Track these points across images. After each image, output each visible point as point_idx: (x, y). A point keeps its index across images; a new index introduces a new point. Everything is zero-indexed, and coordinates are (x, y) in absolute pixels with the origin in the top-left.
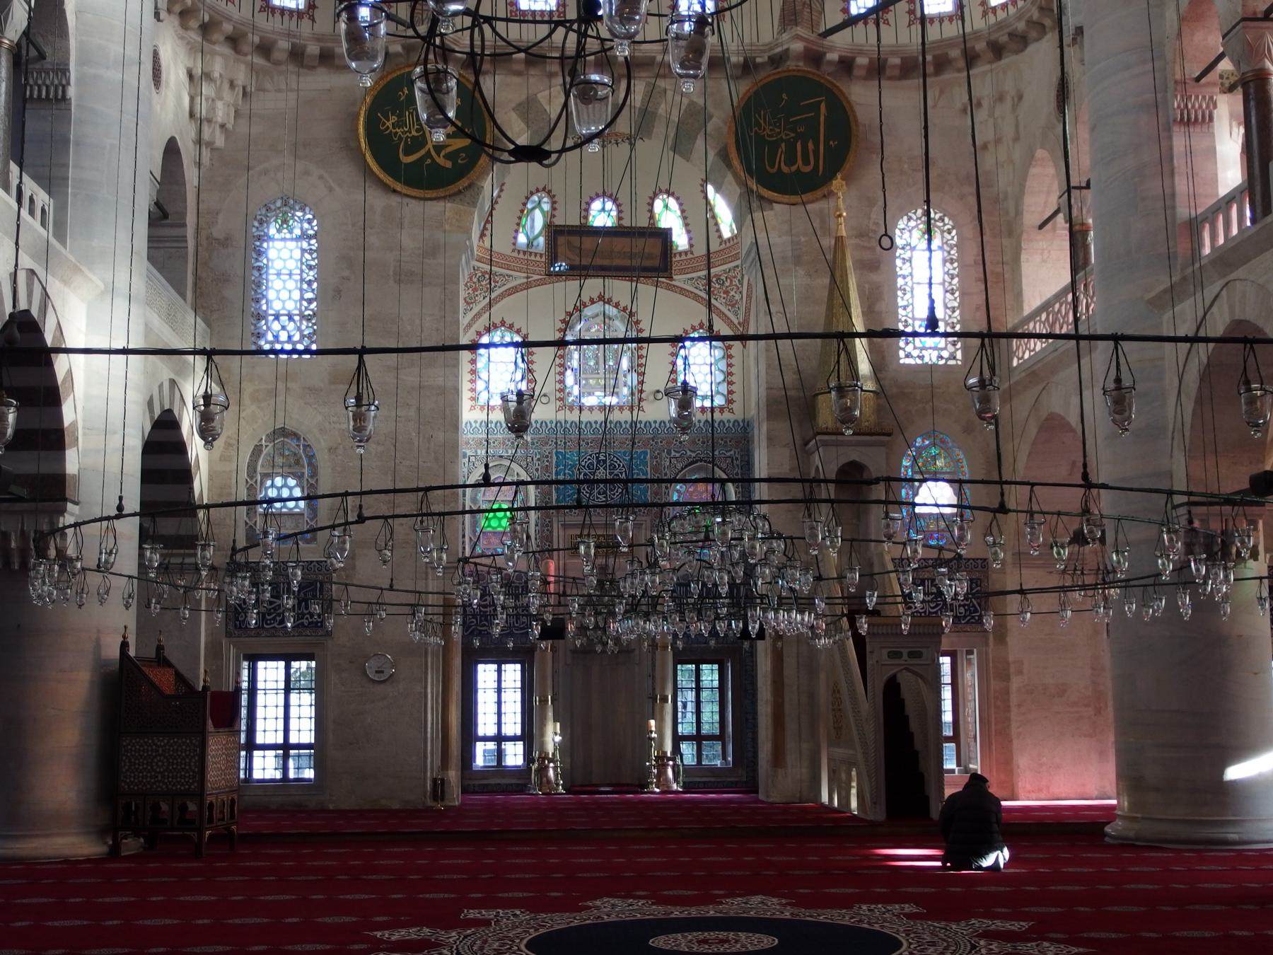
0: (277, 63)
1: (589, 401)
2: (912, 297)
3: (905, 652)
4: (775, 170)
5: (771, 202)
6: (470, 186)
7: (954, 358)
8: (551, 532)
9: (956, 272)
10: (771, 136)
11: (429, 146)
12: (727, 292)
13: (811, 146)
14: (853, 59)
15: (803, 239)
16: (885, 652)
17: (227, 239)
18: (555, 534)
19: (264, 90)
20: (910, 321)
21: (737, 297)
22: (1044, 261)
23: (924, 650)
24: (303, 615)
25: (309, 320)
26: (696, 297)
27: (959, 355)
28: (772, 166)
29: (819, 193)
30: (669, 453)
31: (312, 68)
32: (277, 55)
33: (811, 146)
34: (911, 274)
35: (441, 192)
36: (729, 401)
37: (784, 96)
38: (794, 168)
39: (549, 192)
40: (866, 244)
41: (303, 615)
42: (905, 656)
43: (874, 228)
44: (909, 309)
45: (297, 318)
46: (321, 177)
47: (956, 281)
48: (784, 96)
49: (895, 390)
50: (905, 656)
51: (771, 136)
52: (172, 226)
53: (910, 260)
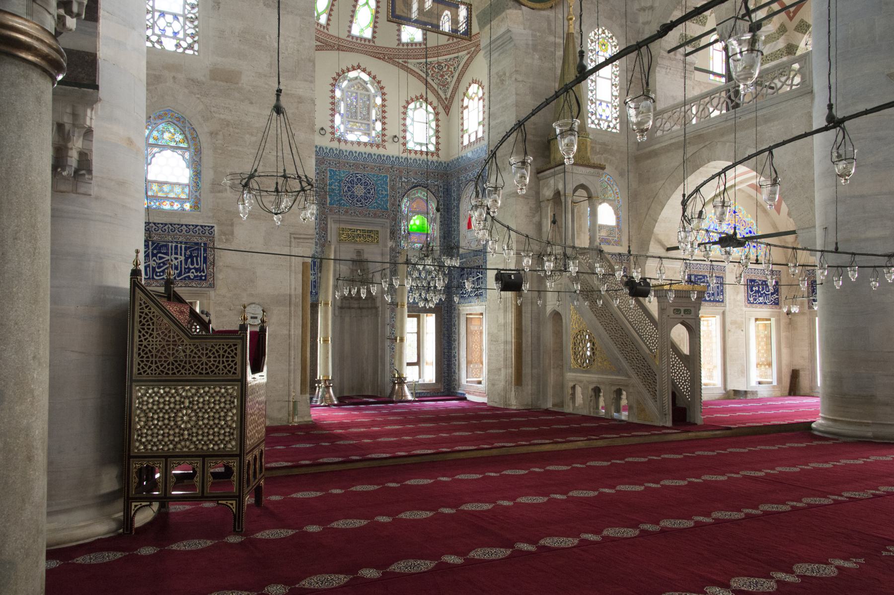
1: (351, 137)
3: (682, 309)
8: (326, 225)
9: (617, 73)
12: (442, 76)
18: (329, 226)
21: (449, 80)
22: (666, 74)
24: (190, 269)
25: (192, 22)
26: (419, 77)
27: (618, 126)
30: (401, 178)
36: (437, 149)
41: (190, 269)
45: (181, 19)
47: (617, 79)
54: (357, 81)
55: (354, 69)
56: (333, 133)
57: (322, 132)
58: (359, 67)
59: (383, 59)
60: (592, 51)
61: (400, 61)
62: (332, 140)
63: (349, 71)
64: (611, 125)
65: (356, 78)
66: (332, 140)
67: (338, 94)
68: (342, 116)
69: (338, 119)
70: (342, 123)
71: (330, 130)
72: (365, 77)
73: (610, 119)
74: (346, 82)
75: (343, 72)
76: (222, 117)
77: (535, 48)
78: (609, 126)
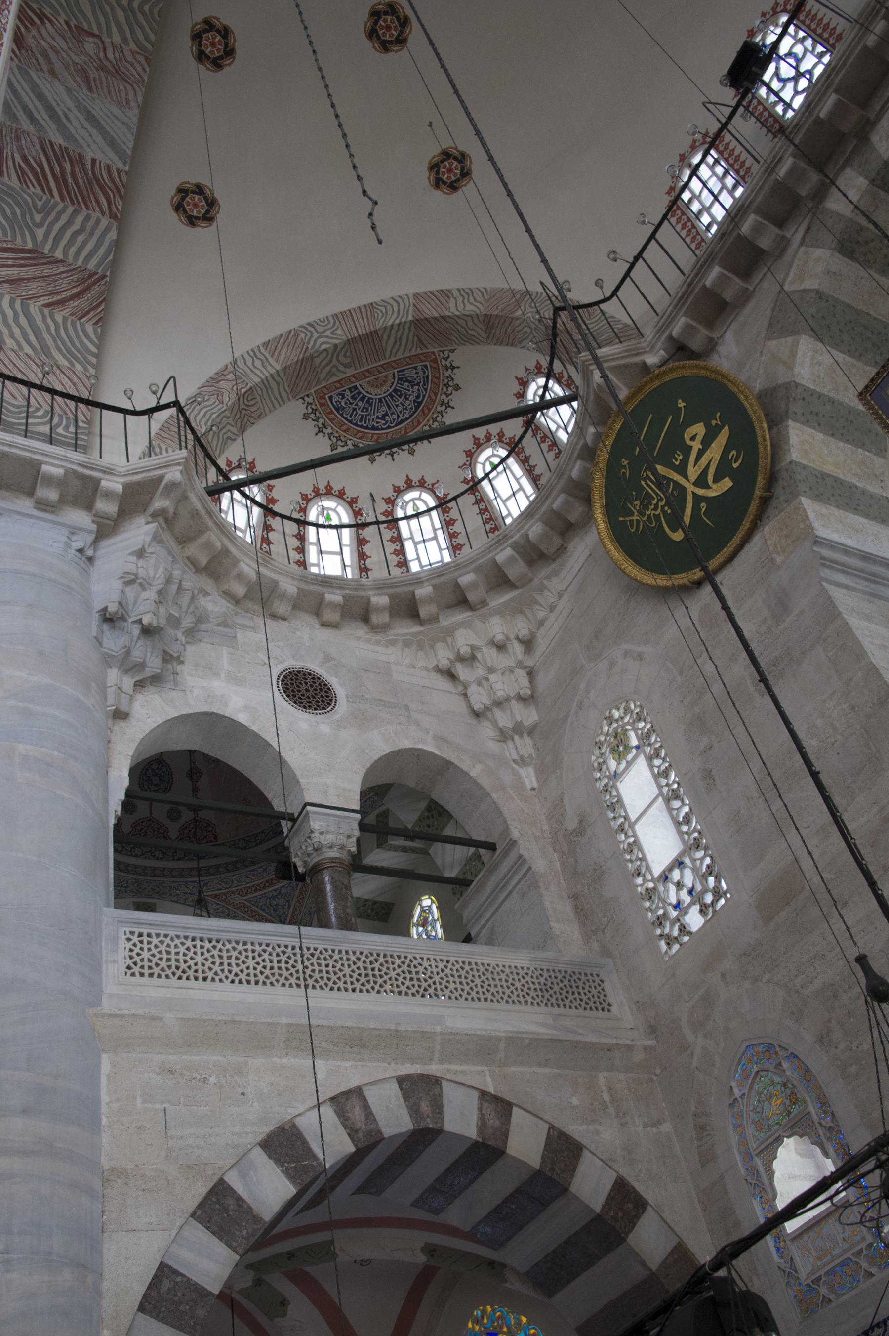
0: (526, 581)
6: (772, 479)
11: (690, 488)
17: (581, 822)
19: (541, 623)
31: (561, 550)
32: (512, 573)
35: (746, 524)
46: (626, 653)
52: (506, 853)
76: (818, 984)
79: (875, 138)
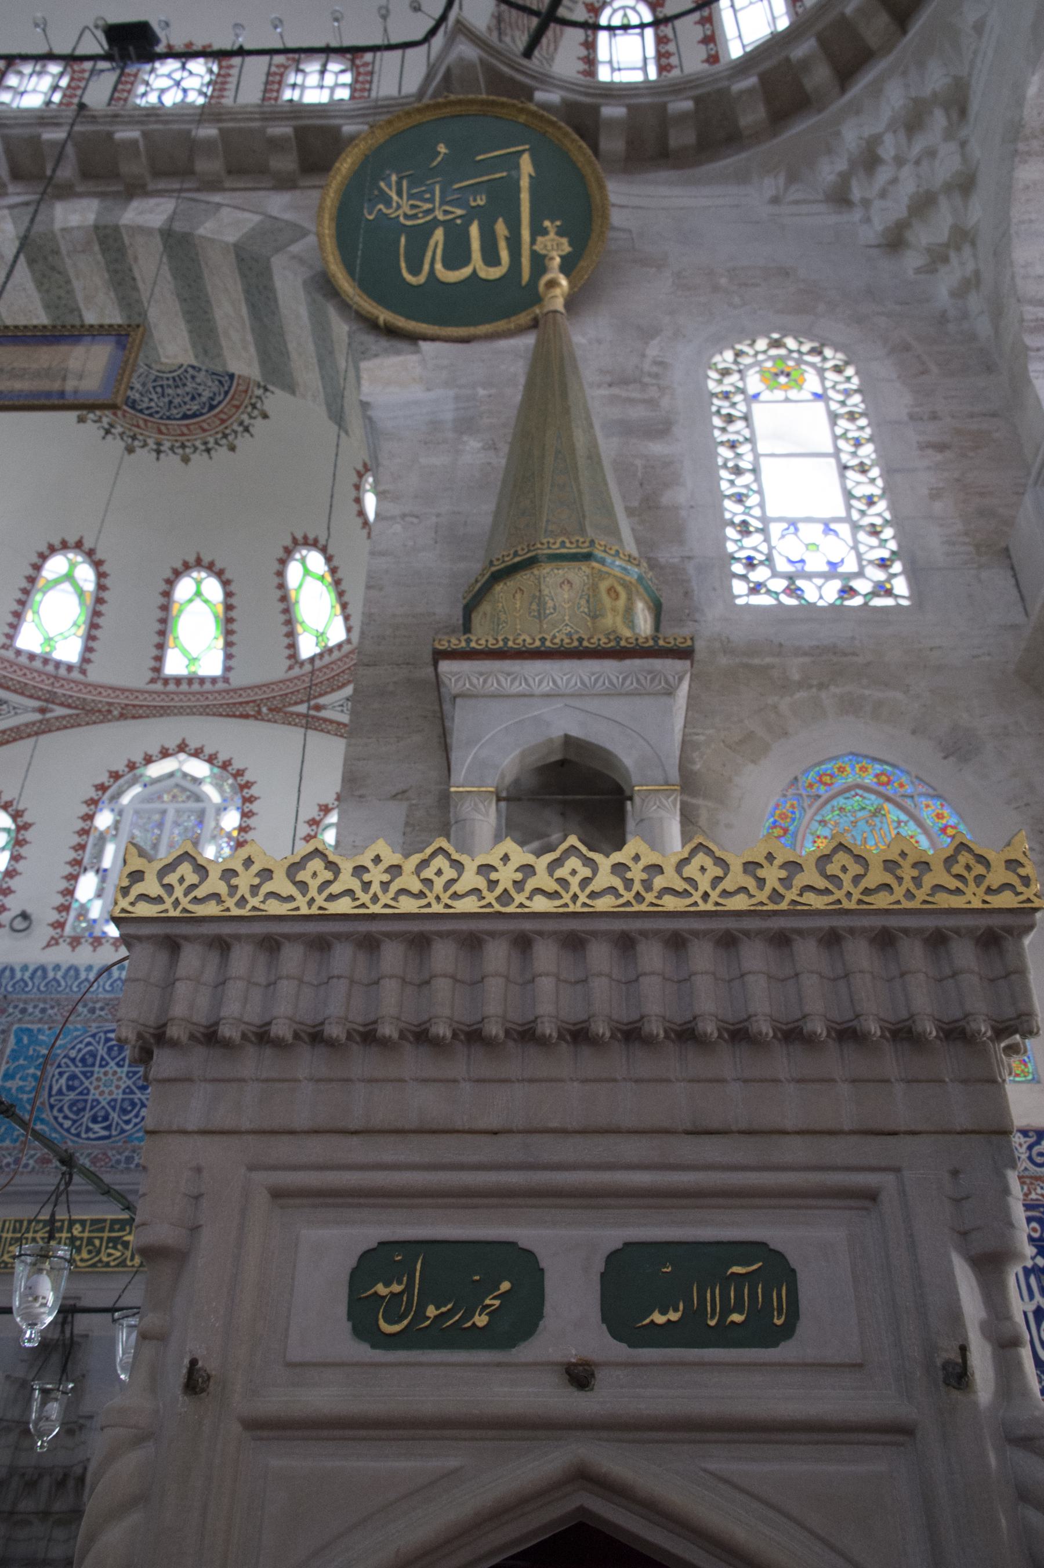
2: (757, 480)
3: (572, 1258)
4: (422, 279)
5: (413, 338)
7: (889, 593)
10: (414, 217)
13: (501, 229)
14: (595, 109)
15: (481, 392)
16: (332, 1246)
20: (755, 524)
23: (815, 1246)
27: (900, 586)
28: (415, 270)
29: (524, 318)
33: (501, 229)
34: (751, 440)
37: (442, 149)
38: (466, 272)
39: (90, 554)
40: (636, 395)
42: (572, 1315)
43: (655, 369)
44: (753, 500)
48: (442, 149)
49: (724, 661)
50: (572, 1315)
51: (414, 217)
53: (746, 418)
54: (171, 782)
55: (165, 754)
56: (60, 925)
57: (19, 924)
58: (182, 748)
59: (258, 716)
60: (726, 396)
61: (302, 708)
62: (53, 942)
63: (149, 760)
64: (863, 586)
65: (171, 775)
66: (53, 942)
67: (104, 820)
68: (103, 874)
69: (87, 886)
70: (99, 894)
71: (54, 916)
72: (198, 768)
73: (850, 566)
74: (137, 789)
75: (132, 766)
77: (465, 425)
78: (848, 591)
79: (135, 204)
